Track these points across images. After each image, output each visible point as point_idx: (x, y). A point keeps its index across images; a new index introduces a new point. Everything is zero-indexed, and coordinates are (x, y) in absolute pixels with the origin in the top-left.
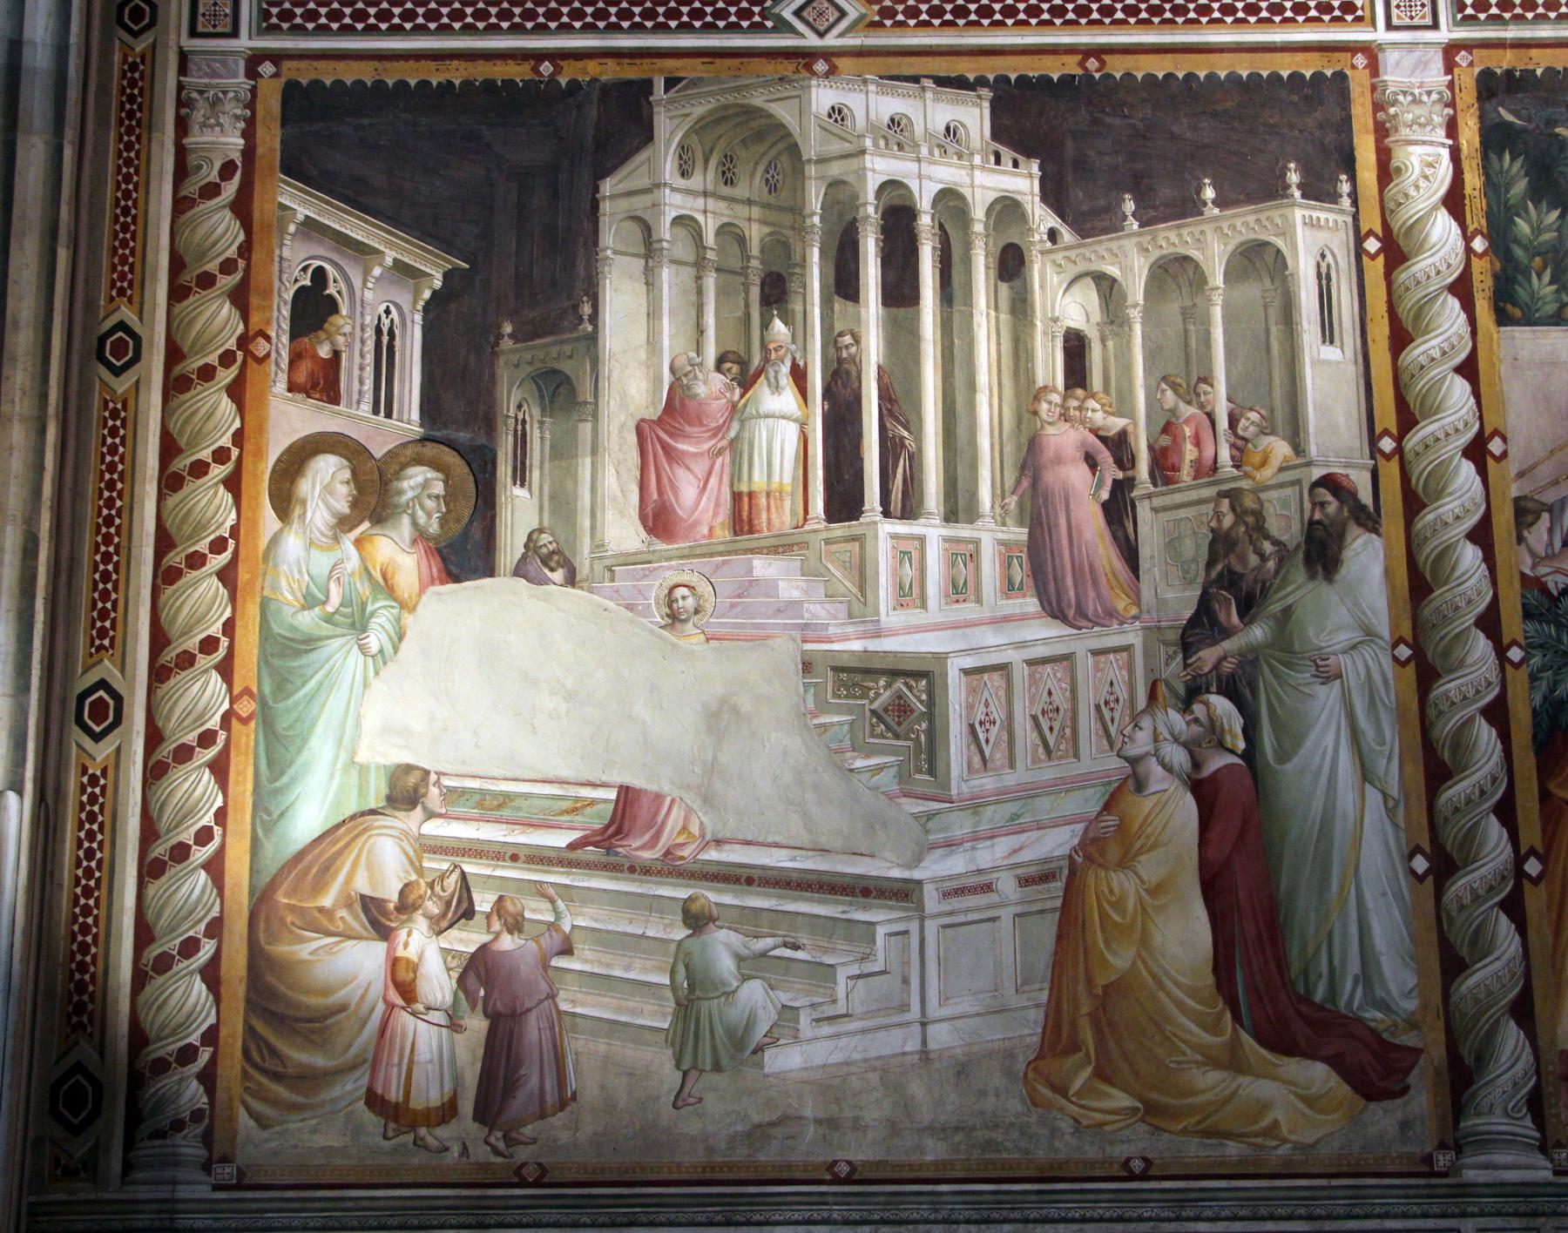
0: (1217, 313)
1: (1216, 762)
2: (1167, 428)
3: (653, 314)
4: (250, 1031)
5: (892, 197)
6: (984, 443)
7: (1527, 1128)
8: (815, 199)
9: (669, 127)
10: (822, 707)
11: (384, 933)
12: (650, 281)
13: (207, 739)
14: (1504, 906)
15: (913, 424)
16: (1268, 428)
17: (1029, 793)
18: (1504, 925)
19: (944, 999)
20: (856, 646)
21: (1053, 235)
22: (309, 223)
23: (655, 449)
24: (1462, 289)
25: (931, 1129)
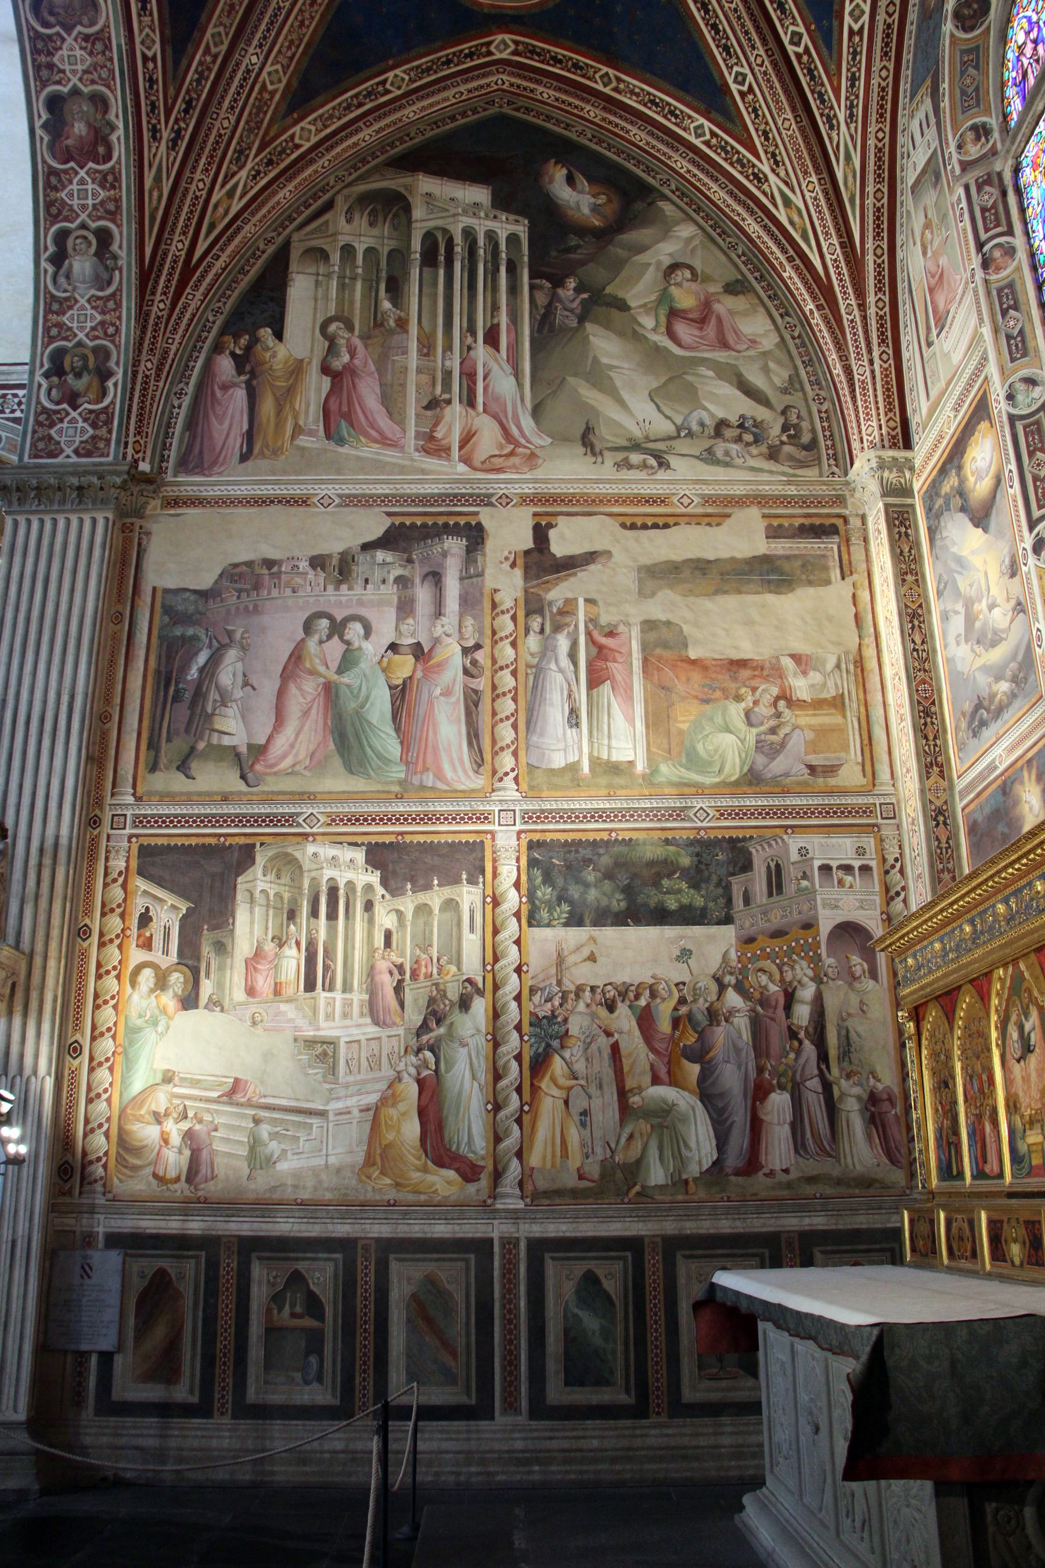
0: (436, 923)
1: (425, 1073)
2: (417, 962)
3: (252, 923)
4: (118, 1153)
5: (331, 883)
6: (356, 967)
7: (518, 1191)
8: (306, 884)
9: (261, 859)
10: (300, 1053)
11: (159, 1123)
12: (252, 912)
13: (107, 1060)
14: (516, 1121)
15: (334, 960)
16: (449, 962)
17: (364, 1082)
18: (516, 1127)
19: (334, 1148)
20: (312, 1033)
21: (383, 896)
22: (145, 891)
23: (251, 967)
24: (517, 915)
25: (327, 1189)
